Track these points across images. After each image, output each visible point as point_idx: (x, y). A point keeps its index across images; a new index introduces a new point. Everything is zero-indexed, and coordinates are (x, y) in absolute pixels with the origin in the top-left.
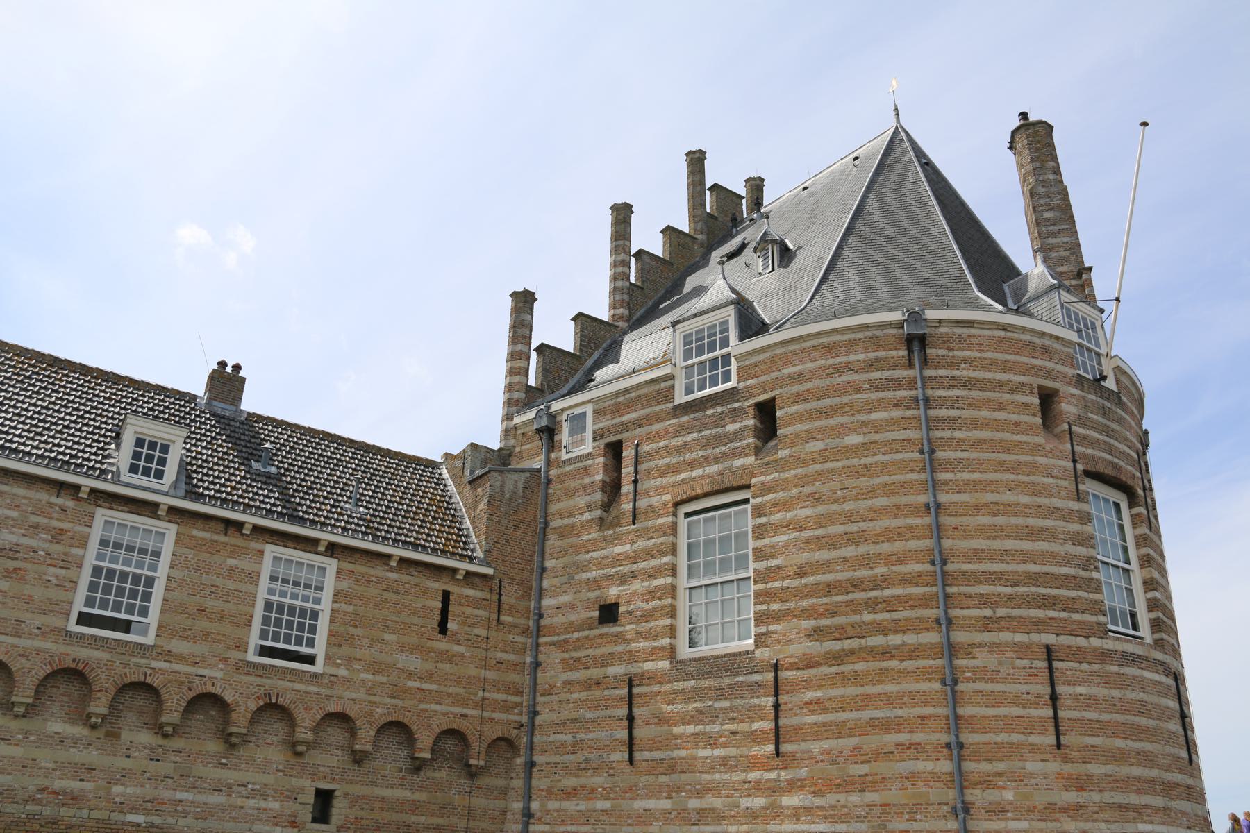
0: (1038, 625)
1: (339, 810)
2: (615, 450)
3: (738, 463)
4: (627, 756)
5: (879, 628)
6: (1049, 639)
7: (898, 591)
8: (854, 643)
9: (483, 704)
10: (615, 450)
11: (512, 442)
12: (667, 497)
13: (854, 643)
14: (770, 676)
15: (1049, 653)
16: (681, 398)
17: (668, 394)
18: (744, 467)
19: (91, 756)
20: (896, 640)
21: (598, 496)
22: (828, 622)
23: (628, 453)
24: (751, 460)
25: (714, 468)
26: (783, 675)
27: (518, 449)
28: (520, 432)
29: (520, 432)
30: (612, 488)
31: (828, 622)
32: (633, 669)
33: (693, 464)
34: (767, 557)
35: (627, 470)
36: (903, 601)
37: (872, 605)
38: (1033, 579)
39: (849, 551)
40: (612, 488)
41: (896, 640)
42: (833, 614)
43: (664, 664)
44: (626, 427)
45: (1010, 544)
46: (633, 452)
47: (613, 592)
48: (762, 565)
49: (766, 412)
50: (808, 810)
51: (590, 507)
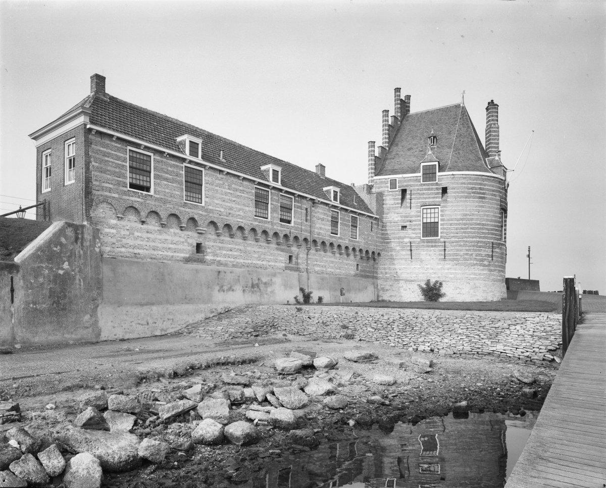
0: (491, 238)
1: (360, 268)
2: (404, 192)
3: (437, 200)
4: (410, 257)
5: (466, 237)
6: (492, 241)
7: (470, 230)
8: (461, 239)
9: (377, 246)
10: (404, 192)
11: (373, 184)
12: (419, 204)
13: (461, 239)
14: (443, 244)
15: (492, 242)
16: (422, 182)
17: (420, 181)
18: (439, 201)
19: (333, 259)
20: (469, 239)
21: (400, 201)
22: (456, 235)
23: (408, 192)
24: (440, 200)
25: (432, 200)
26: (446, 244)
27: (375, 186)
28: (375, 181)
29: (375, 181)
30: (403, 198)
31: (456, 235)
32: (411, 240)
33: (425, 198)
34: (443, 221)
35: (408, 196)
36: (470, 232)
37: (465, 233)
38: (492, 230)
39: (461, 222)
40: (403, 198)
41: (469, 239)
42: (457, 234)
43: (419, 240)
44: (406, 186)
45: (489, 223)
46: (410, 192)
47: (405, 224)
48: (443, 222)
49: (445, 190)
50: (451, 268)
51: (398, 204)
